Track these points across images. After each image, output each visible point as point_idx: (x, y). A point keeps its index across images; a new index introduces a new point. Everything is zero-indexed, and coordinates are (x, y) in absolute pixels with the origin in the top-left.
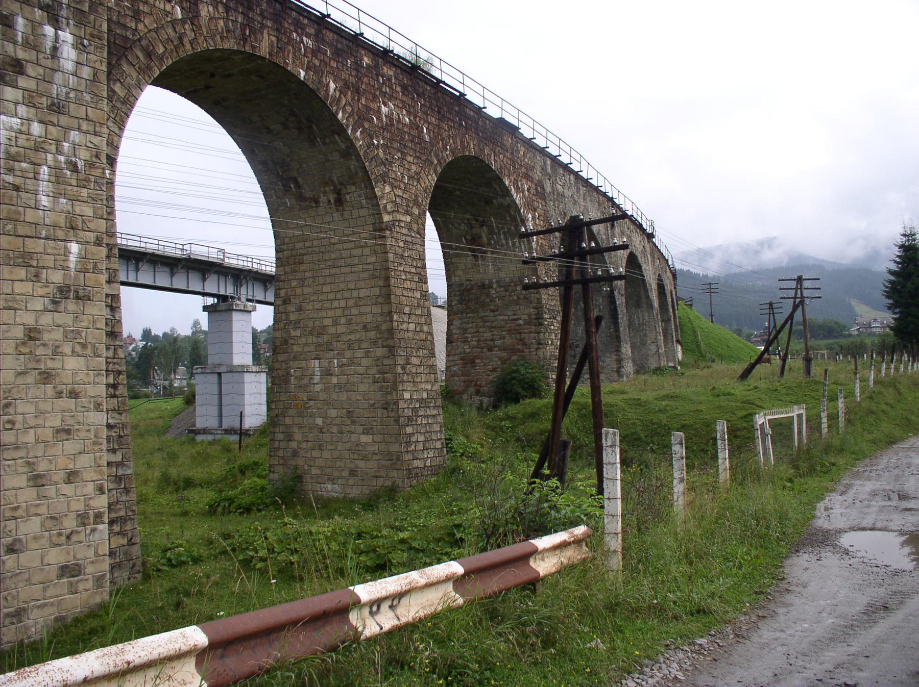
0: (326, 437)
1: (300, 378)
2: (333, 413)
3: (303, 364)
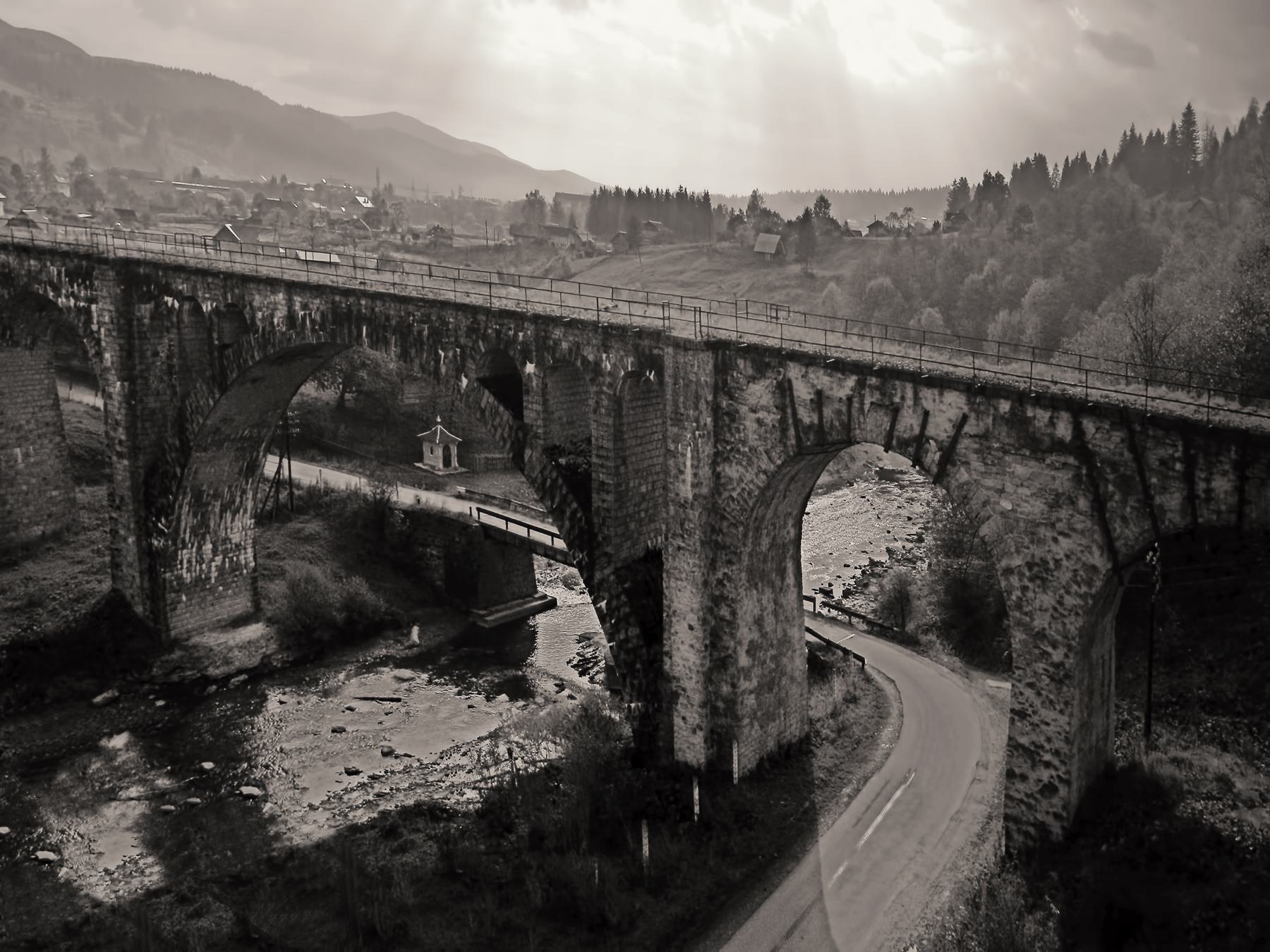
0: (30, 496)
1: (7, 462)
2: (34, 481)
3: (9, 451)
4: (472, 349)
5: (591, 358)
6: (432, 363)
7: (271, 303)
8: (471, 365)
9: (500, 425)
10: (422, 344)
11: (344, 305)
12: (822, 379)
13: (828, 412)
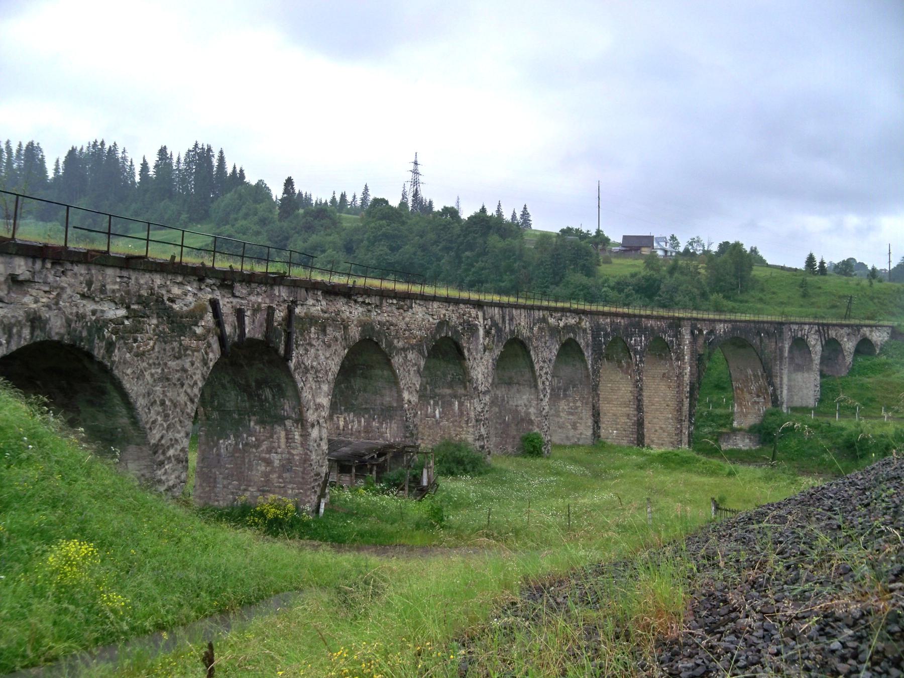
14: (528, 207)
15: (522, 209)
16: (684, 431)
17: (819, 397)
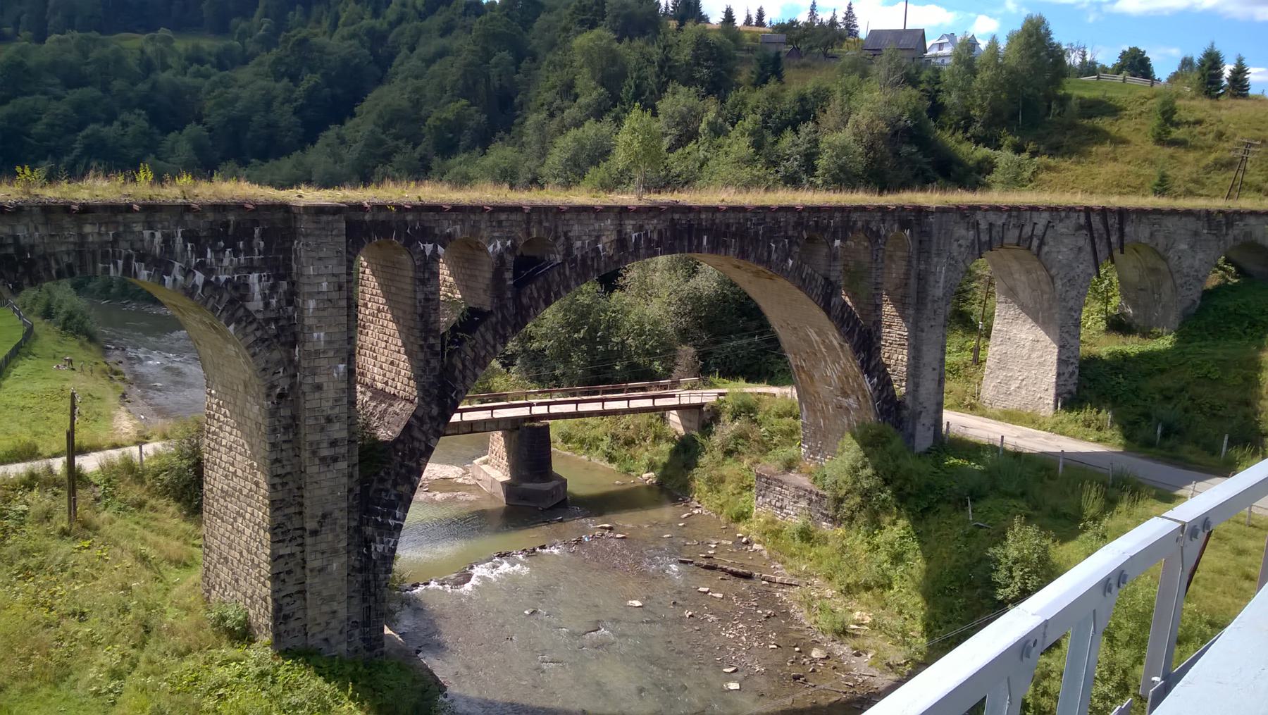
4: (798, 237)
5: (874, 229)
6: (766, 254)
7: (594, 230)
8: (796, 249)
9: (816, 286)
10: (757, 240)
11: (684, 222)
12: (992, 217)
13: (994, 233)
14: (852, 6)
15: (846, 10)
16: (314, 562)
17: (1074, 389)
